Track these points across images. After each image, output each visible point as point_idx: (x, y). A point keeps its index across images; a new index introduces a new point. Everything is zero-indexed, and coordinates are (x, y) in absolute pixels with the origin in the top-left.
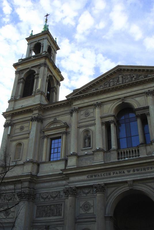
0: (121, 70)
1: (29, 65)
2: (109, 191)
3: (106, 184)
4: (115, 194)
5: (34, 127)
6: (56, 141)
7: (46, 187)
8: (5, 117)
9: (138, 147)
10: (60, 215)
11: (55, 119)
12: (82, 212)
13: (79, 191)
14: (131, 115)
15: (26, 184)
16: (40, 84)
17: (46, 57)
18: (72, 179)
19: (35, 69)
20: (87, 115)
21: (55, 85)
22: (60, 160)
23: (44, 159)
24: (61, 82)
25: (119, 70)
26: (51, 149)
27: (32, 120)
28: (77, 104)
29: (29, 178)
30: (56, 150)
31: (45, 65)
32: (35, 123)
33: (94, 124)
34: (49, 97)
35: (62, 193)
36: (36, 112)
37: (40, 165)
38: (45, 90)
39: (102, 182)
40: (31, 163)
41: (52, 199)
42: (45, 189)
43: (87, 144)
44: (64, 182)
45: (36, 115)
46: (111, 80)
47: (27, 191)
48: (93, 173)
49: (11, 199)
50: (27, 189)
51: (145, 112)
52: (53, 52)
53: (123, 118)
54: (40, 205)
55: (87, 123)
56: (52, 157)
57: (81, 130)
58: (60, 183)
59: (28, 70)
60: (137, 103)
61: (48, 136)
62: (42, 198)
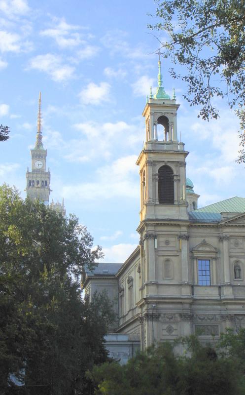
7: (202, 310)
18: (229, 307)
19: (173, 167)
29: (191, 301)
40: (189, 287)
41: (209, 321)
42: (201, 311)
49: (172, 317)
50: (189, 311)
54: (197, 325)
55: (238, 254)
57: (233, 260)
58: (215, 307)
59: (163, 164)
61: (197, 258)
62: (200, 319)
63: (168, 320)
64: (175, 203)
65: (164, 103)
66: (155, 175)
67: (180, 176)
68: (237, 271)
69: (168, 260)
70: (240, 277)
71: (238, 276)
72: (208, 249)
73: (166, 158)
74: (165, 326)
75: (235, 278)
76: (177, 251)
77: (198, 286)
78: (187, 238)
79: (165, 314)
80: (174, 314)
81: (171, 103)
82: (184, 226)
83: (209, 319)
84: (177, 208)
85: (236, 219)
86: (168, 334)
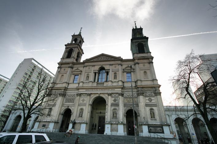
1: (71, 46)
2: (92, 96)
3: (91, 93)
4: (93, 97)
5: (69, 70)
6: (77, 76)
8: (59, 64)
9: (104, 82)
10: (74, 102)
11: (78, 68)
12: (82, 102)
13: (82, 95)
14: (104, 71)
15: (63, 90)
16: (74, 54)
17: (78, 45)
18: (80, 90)
19: (73, 48)
21: (80, 56)
22: (77, 83)
23: (71, 83)
24: (83, 55)
25: (103, 55)
26: (74, 79)
27: (69, 67)
28: (86, 64)
30: (76, 80)
31: (77, 47)
32: (70, 69)
33: (91, 72)
34: (77, 60)
35: (76, 95)
36: (71, 65)
37: (70, 84)
38: (76, 57)
39: (90, 92)
43: (87, 79)
44: (77, 91)
45: (71, 66)
47: (63, 93)
48: (87, 89)
52: (81, 43)
53: (101, 72)
56: (74, 81)
57: (86, 74)
58: (76, 91)
60: (107, 67)
61: (74, 74)
72: (79, 71)
83: (72, 96)
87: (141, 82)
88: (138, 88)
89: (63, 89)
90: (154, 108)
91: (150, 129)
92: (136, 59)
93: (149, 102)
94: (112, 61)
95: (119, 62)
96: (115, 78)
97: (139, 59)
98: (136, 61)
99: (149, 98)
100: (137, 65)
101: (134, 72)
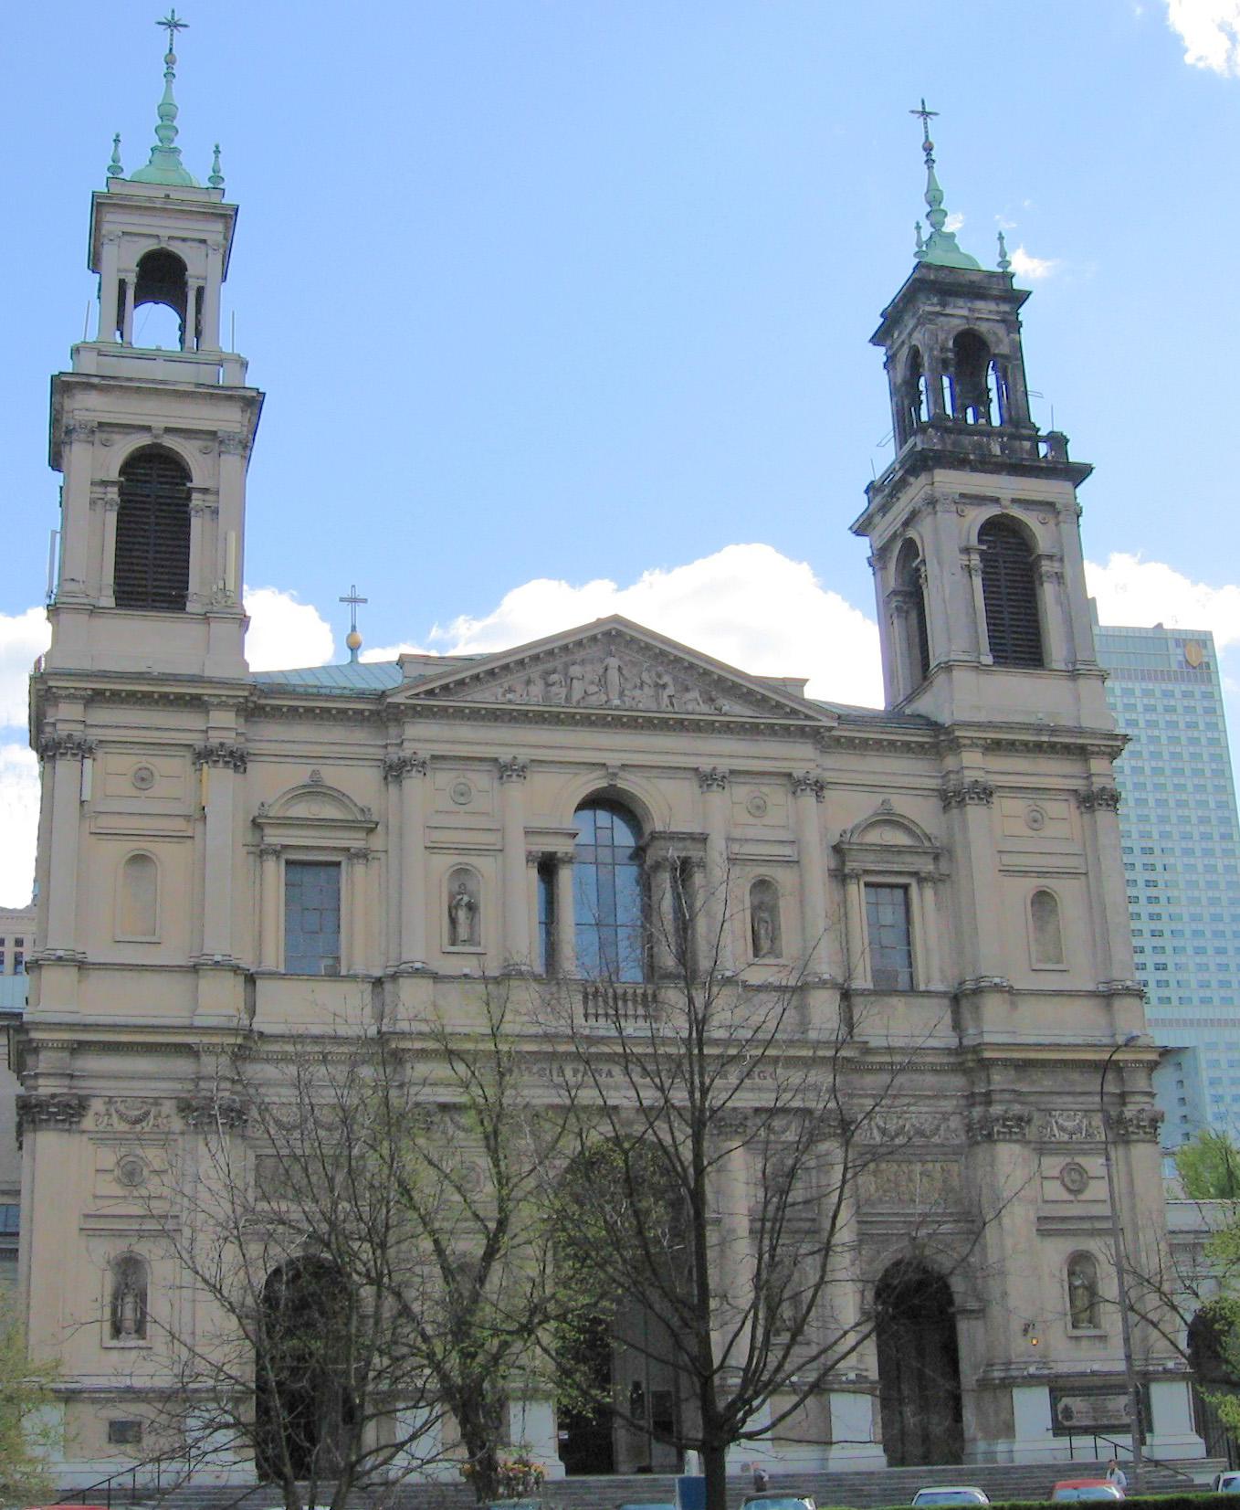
0: (620, 634)
19: (188, 451)
20: (462, 800)
28: (422, 737)
29: (239, 1041)
46: (575, 670)
49: (147, 1114)
51: (694, 853)
59: (144, 440)
60: (671, 806)
63: (123, 1127)
64: (190, 607)
65: (167, 196)
66: (104, 483)
67: (217, 493)
68: (462, 914)
69: (139, 859)
70: (471, 941)
71: (463, 932)
72: (329, 811)
73: (159, 414)
74: (108, 1158)
75: (453, 944)
76: (187, 817)
77: (272, 975)
78: (238, 760)
79: (110, 1100)
80: (157, 1102)
81: (203, 198)
82: (222, 705)
84: (197, 630)
85: (461, 683)
86: (119, 1191)
87: (1014, 1006)
88: (986, 1065)
89: (211, 1050)
90: (1093, 1245)
91: (1061, 1406)
92: (973, 744)
93: (1067, 1196)
94: (728, 729)
95: (801, 757)
96: (765, 945)
97: (995, 747)
98: (974, 765)
99: (1068, 1160)
100: (974, 812)
101: (937, 880)
